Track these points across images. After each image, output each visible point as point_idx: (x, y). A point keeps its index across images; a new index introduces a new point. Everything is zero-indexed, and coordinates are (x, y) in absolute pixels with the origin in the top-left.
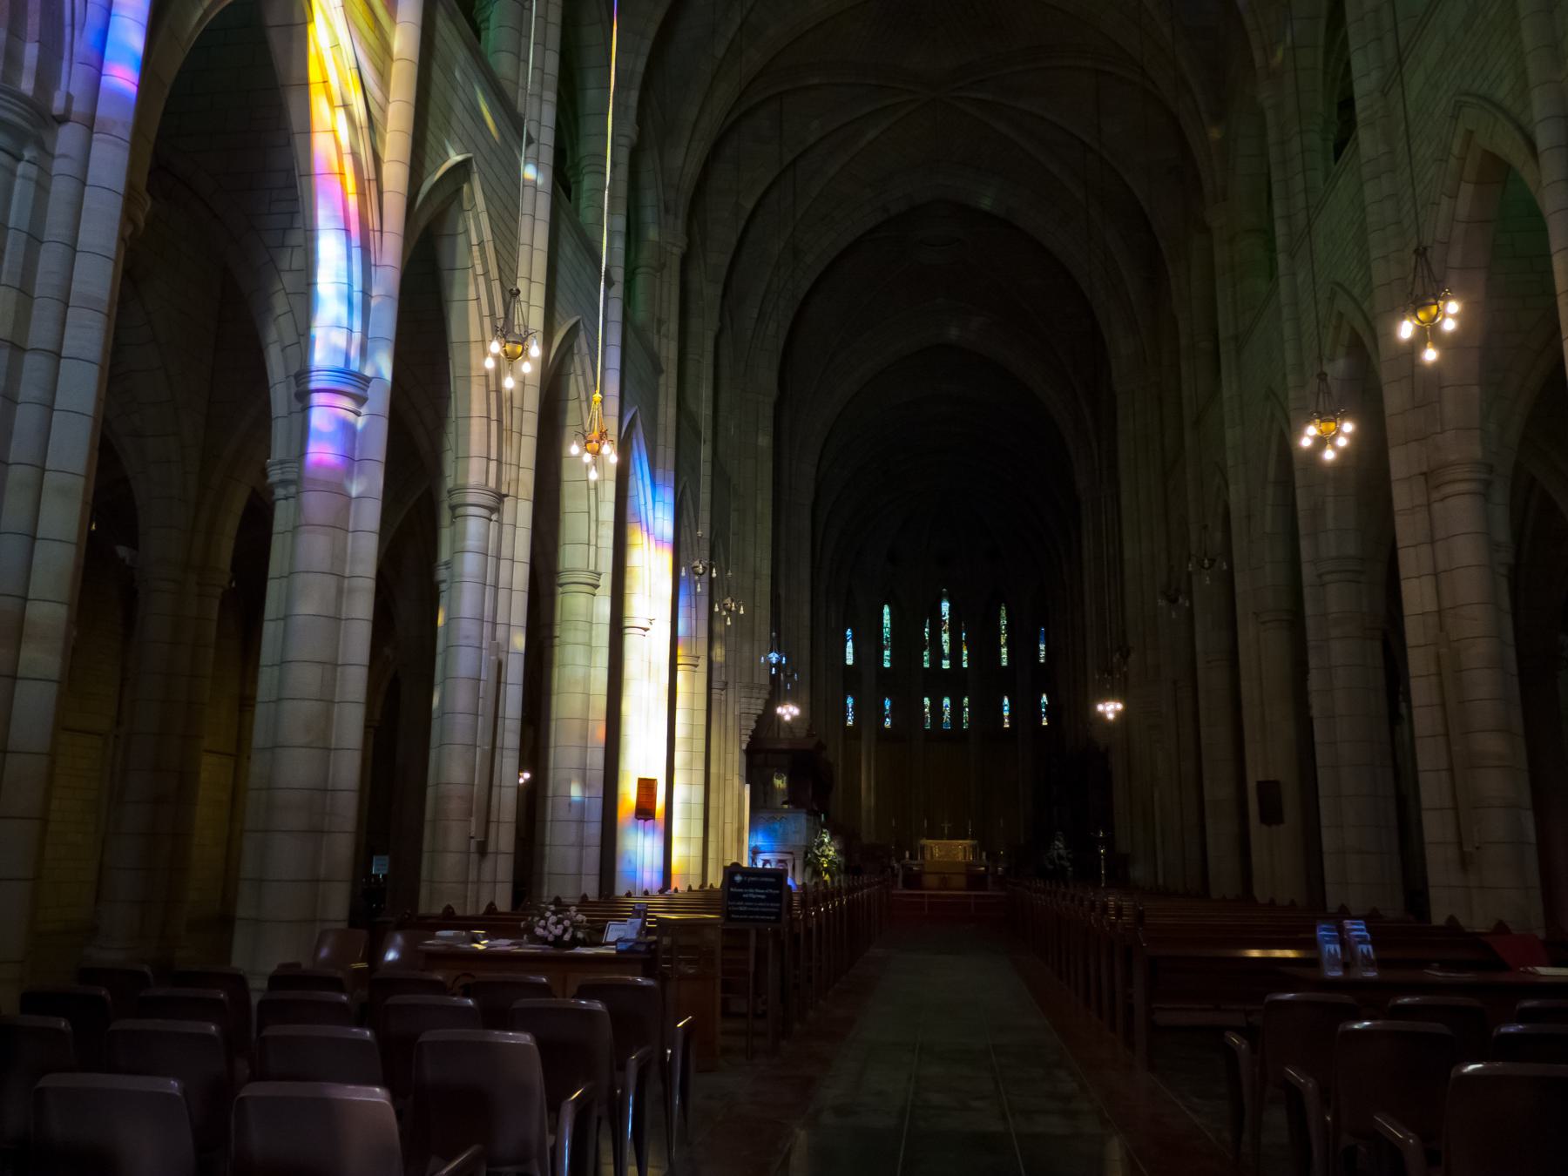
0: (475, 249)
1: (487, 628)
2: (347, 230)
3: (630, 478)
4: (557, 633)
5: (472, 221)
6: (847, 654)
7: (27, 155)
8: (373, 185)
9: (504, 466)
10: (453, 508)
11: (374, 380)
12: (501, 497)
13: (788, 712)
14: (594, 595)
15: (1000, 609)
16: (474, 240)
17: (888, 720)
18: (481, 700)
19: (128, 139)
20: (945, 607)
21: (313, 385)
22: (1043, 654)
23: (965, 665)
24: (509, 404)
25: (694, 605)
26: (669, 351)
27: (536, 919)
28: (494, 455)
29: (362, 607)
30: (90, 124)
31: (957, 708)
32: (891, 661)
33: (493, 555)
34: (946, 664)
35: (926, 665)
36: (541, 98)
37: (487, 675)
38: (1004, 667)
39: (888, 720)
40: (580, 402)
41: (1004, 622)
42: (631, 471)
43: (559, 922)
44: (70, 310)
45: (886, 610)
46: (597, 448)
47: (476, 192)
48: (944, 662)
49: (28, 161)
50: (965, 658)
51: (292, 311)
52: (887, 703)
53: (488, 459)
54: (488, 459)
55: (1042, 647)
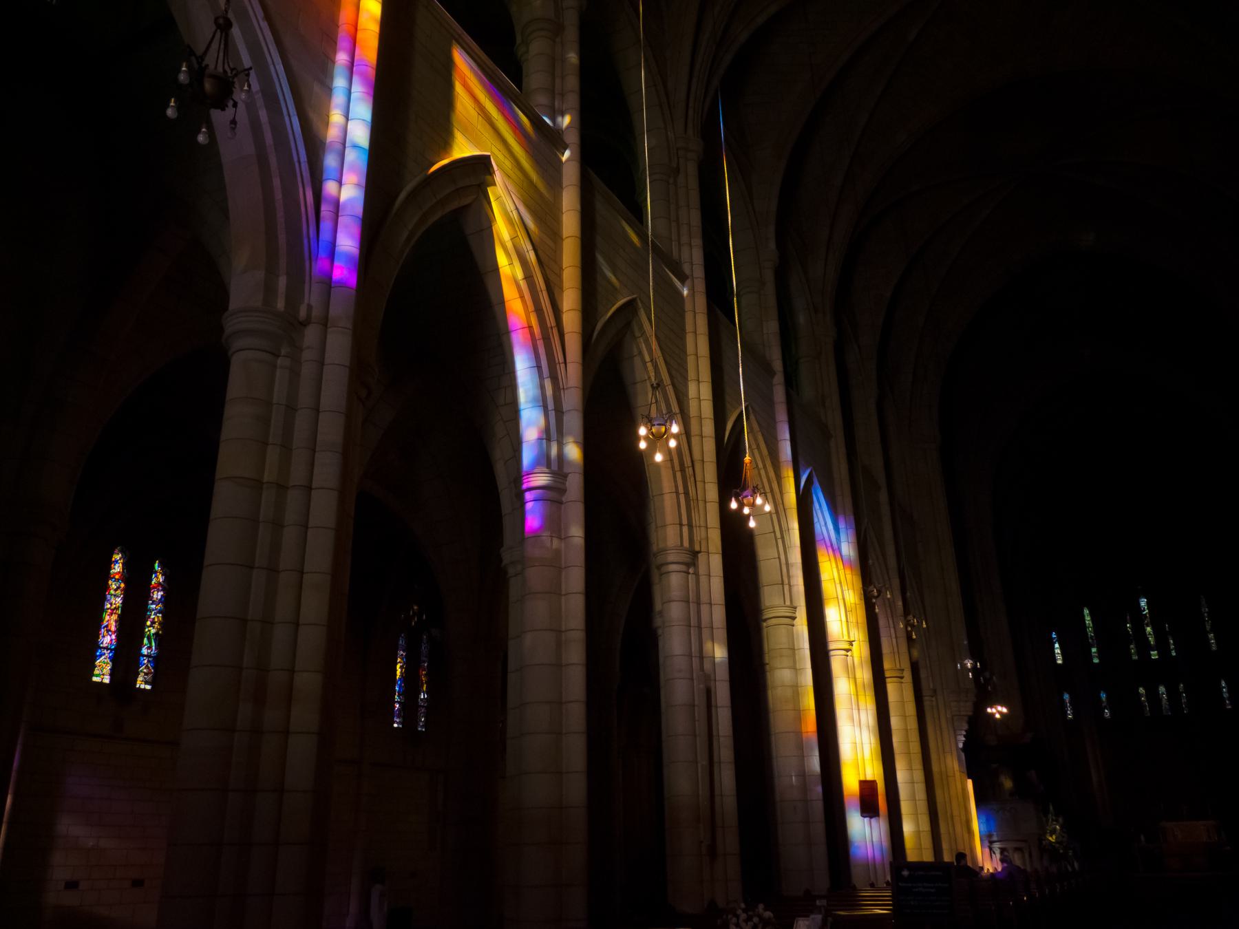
0: (649, 365)
1: (695, 661)
2: (539, 367)
3: (815, 525)
4: (767, 660)
5: (643, 344)
7: (283, 352)
8: (555, 331)
9: (694, 529)
10: (659, 567)
11: (570, 475)
12: (695, 554)
13: (998, 711)
14: (793, 625)
16: (647, 358)
18: (697, 723)
19: (351, 328)
20: (1143, 603)
21: (525, 486)
24: (692, 479)
25: (892, 625)
26: (834, 419)
27: (725, 917)
28: (685, 521)
29: (576, 655)
30: (325, 322)
31: (1173, 692)
32: (1099, 657)
33: (694, 601)
34: (1154, 655)
35: (1135, 657)
36: (690, 245)
37: (700, 701)
39: (1106, 711)
40: (759, 470)
42: (816, 520)
43: (749, 919)
44: (317, 455)
45: (1086, 611)
46: (752, 501)
47: (647, 325)
49: (284, 356)
50: (1172, 647)
51: (508, 434)
52: (1103, 696)
53: (681, 525)
54: (681, 525)
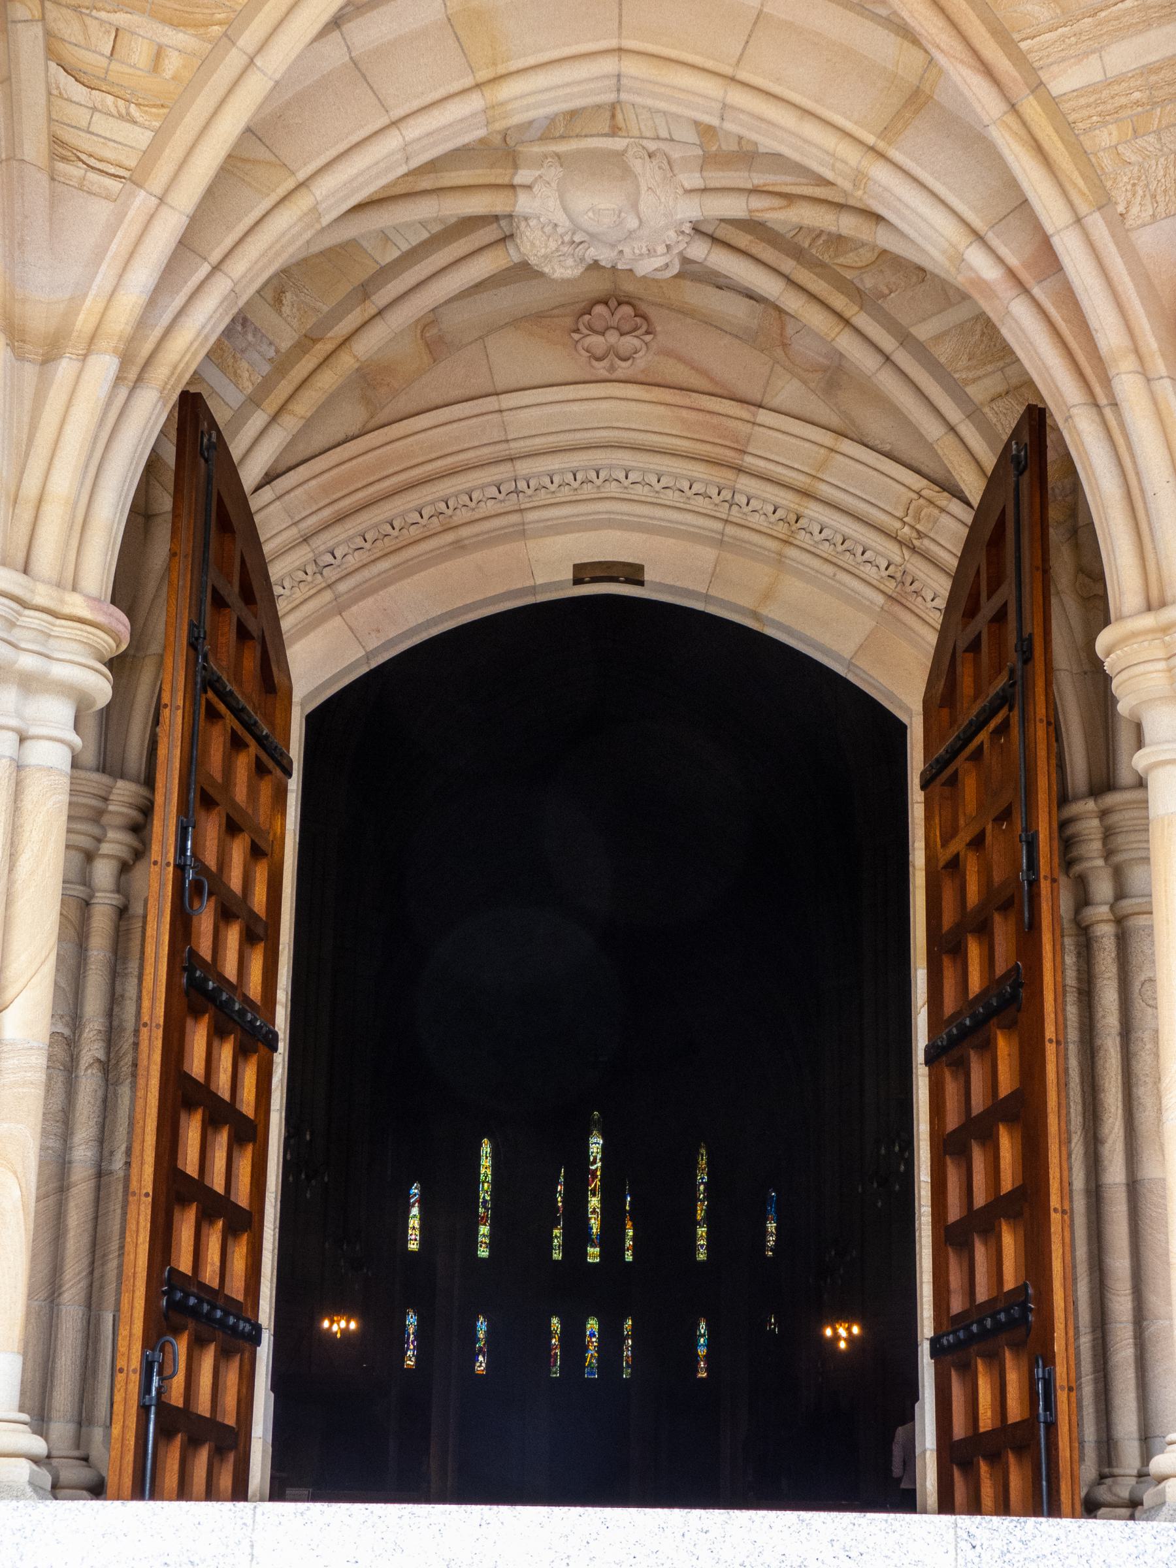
6: (410, 1232)
13: (339, 1326)
15: (698, 1153)
17: (481, 1358)
20: (596, 1145)
22: (771, 1241)
23: (629, 1257)
31: (611, 1338)
32: (491, 1246)
34: (593, 1254)
38: (702, 1262)
41: (702, 1177)
45: (486, 1148)
48: (590, 1250)
50: (629, 1243)
55: (771, 1226)
